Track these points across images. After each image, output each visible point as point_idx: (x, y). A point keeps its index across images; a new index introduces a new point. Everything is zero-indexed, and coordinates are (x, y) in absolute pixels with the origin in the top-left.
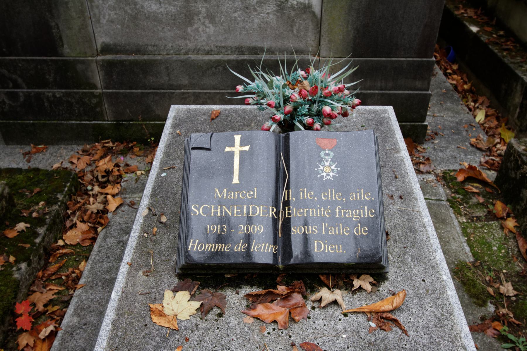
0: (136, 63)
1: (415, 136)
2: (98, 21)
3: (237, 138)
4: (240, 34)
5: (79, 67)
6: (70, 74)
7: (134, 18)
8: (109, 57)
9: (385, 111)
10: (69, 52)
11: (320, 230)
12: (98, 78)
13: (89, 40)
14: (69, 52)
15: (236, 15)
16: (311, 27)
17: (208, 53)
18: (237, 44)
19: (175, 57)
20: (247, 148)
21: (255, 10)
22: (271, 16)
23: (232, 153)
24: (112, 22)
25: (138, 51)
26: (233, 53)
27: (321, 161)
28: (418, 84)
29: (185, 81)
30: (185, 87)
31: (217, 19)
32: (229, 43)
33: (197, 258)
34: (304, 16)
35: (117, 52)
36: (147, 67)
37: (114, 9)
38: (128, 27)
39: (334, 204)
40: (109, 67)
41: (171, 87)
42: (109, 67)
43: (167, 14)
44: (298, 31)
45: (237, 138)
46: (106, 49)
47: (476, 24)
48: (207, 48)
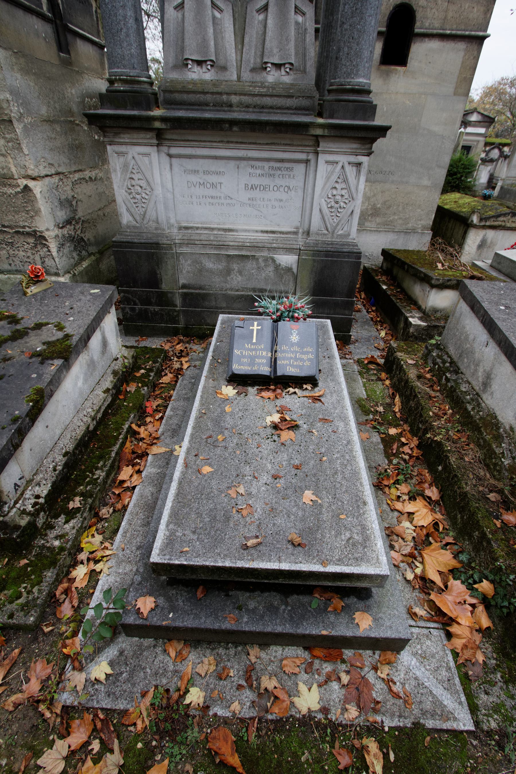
0: (199, 294)
1: (343, 339)
2: (182, 272)
3: (256, 323)
5: (169, 295)
6: (164, 299)
7: (200, 271)
8: (185, 291)
9: (326, 322)
10: (165, 287)
11: (290, 362)
12: (178, 301)
13: (176, 281)
14: (165, 287)
16: (292, 279)
17: (237, 291)
19: (220, 292)
20: (260, 328)
23: (253, 330)
24: (189, 272)
27: (292, 334)
28: (347, 312)
29: (224, 305)
30: (224, 308)
32: (249, 286)
33: (236, 372)
35: (189, 288)
36: (205, 297)
37: (190, 265)
39: (297, 352)
40: (185, 296)
41: (217, 308)
42: (185, 296)
44: (285, 281)
45: (256, 323)
46: (184, 286)
47: (385, 284)
48: (237, 288)
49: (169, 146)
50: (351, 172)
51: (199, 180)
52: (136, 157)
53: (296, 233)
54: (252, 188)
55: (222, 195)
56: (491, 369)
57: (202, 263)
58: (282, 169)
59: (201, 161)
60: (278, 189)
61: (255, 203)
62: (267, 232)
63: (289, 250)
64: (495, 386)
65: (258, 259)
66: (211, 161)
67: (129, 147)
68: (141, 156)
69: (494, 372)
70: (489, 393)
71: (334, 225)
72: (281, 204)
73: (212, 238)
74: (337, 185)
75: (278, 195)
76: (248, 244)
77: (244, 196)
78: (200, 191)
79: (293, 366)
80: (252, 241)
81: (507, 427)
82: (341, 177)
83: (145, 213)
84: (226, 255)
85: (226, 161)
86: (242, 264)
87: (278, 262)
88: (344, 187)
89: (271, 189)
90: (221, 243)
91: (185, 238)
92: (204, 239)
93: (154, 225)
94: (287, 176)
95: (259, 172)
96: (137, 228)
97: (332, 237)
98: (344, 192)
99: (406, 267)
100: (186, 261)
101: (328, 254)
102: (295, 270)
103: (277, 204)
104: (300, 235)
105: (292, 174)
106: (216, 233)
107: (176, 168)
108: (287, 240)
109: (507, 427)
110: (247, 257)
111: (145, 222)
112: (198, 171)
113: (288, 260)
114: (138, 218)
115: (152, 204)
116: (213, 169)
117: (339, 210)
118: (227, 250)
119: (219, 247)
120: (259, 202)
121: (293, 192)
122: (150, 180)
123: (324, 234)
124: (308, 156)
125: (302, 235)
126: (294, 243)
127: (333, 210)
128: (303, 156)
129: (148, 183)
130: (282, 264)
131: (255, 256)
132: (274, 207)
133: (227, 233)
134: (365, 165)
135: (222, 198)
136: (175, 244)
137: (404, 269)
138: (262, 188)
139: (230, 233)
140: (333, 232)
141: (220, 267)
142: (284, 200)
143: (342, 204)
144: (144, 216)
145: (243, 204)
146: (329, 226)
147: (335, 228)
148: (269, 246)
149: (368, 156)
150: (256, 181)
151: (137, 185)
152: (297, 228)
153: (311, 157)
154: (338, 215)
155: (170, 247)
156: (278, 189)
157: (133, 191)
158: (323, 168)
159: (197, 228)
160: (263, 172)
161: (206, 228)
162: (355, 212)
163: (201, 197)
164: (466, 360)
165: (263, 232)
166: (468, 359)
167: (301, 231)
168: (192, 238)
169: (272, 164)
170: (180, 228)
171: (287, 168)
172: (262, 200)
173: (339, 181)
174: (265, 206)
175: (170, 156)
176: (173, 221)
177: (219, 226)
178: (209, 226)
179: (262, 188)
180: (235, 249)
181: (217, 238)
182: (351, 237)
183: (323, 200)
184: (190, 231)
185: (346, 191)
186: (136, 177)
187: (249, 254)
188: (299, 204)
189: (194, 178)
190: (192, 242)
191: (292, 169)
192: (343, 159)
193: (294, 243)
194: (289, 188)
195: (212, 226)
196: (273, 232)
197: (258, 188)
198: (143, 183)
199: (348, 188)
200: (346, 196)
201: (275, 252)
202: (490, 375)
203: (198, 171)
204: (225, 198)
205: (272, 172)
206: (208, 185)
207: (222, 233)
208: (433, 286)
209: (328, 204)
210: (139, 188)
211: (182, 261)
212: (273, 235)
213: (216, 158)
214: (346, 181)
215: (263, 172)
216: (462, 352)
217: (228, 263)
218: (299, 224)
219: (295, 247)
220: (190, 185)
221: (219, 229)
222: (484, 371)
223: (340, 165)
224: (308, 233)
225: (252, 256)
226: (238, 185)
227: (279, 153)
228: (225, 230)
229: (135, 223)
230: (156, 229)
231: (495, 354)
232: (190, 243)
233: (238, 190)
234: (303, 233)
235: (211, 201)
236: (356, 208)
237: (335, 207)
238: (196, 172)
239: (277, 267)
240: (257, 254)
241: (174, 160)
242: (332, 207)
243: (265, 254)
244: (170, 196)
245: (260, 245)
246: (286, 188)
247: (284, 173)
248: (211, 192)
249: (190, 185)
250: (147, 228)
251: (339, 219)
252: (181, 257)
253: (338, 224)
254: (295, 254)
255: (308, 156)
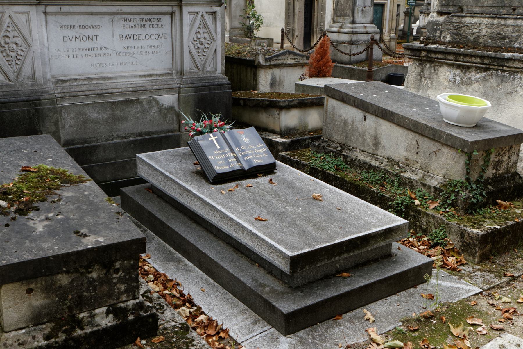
0: (92, 147)
2: (63, 127)
4: (141, 125)
7: (85, 123)
15: (138, 115)
16: (175, 118)
17: (125, 138)
18: (139, 131)
19: (108, 142)
21: (147, 111)
22: (156, 114)
24: (72, 126)
25: (85, 142)
26: (137, 136)
29: (113, 155)
30: (114, 159)
31: (129, 119)
32: (135, 131)
34: (171, 112)
35: (73, 144)
37: (74, 119)
38: (80, 129)
43: (103, 119)
44: (169, 120)
48: (124, 135)
49: (46, 5)
50: (209, 19)
51: (74, 34)
52: (13, 15)
53: (170, 74)
54: (126, 38)
55: (99, 47)
56: (376, 132)
57: (86, 115)
58: (152, 20)
59: (77, 17)
60: (150, 37)
61: (130, 51)
62: (144, 76)
63: (169, 90)
64: (383, 141)
65: (142, 102)
66: (86, 16)
67: (5, 7)
68: (17, 15)
69: (379, 132)
70: (381, 148)
71: (203, 63)
72: (154, 50)
73: (92, 88)
74: (199, 30)
75: (150, 42)
76: (131, 89)
77: (119, 46)
78: (76, 44)
79: (258, 159)
80: (133, 86)
81: (404, 160)
82: (202, 23)
83: (20, 70)
84: (111, 102)
85: (101, 16)
86: (127, 110)
87: (160, 103)
88: (206, 31)
89: (144, 37)
90: (104, 92)
91: (65, 91)
92: (85, 89)
93: (30, 82)
94: (156, 26)
95: (131, 23)
96: (11, 86)
97: (203, 73)
98: (206, 35)
99: (242, 102)
100: (69, 114)
101: (203, 88)
102: (176, 108)
103: (150, 50)
104: (174, 76)
105: (160, 24)
106: (95, 82)
107: (51, 26)
108: (165, 81)
109: (404, 160)
110: (131, 101)
111: (20, 80)
112: (74, 26)
113: (169, 99)
114: (12, 76)
115: (28, 61)
116: (89, 23)
117: (205, 50)
118: (110, 97)
119: (103, 95)
120: (133, 50)
121: (163, 39)
122: (27, 37)
123: (196, 72)
124: (173, 9)
125: (176, 76)
126: (171, 82)
127: (200, 51)
128: (169, 9)
129: (24, 39)
130: (164, 103)
131: (139, 99)
132: (147, 53)
133: (107, 82)
134: (219, 13)
135: (99, 49)
136: (57, 98)
137: (239, 104)
138: (135, 37)
139: (110, 81)
140: (203, 69)
141: (105, 116)
142: (156, 46)
143: (207, 45)
144: (18, 74)
145: (118, 53)
146: (199, 65)
147: (204, 65)
148: (150, 88)
149: (220, 6)
150: (129, 32)
151: (12, 43)
152: (170, 70)
153: (176, 9)
154: (204, 54)
155: (53, 101)
156: (150, 37)
157: (7, 49)
158: (187, 18)
159: (76, 80)
160: (135, 24)
161: (84, 79)
162: (217, 50)
163: (77, 50)
164: (352, 138)
165: (140, 76)
166: (354, 136)
167: (174, 72)
168: (72, 90)
169: (142, 16)
170: (57, 82)
171: (156, 20)
172: (136, 47)
173: (201, 26)
174: (139, 53)
175: (45, 13)
176: (48, 76)
177: (97, 76)
178: (87, 76)
179: (135, 37)
180: (119, 95)
181: (98, 87)
182: (218, 72)
183: (191, 43)
184: (68, 84)
185: (207, 34)
186: (11, 35)
187: (132, 98)
188: (169, 49)
189: (70, 33)
190: (74, 94)
191: (160, 20)
192: (202, 10)
193: (171, 82)
194: (159, 35)
195: (91, 76)
196: (150, 76)
197: (132, 38)
198: (19, 41)
199: (209, 32)
200: (208, 38)
201: (157, 93)
202: (377, 136)
203: (74, 26)
204: (102, 49)
205: (142, 23)
206: (85, 39)
207: (102, 82)
208: (281, 108)
209: (194, 46)
210: (15, 46)
211: (64, 115)
212: (151, 79)
213: (92, 14)
214: (206, 26)
215: (135, 24)
216: (347, 133)
217: (113, 111)
218: (171, 66)
219: (174, 86)
220: (65, 39)
221: (98, 79)
222: (371, 136)
223: (200, 14)
224: (181, 73)
225: (137, 99)
226: (113, 36)
227: (165, 7)
228: (104, 79)
229: (7, 81)
230: (33, 85)
231: (374, 121)
232: (72, 95)
233: (113, 40)
234: (177, 73)
235: (88, 52)
236: (218, 47)
237: (202, 48)
238: (72, 27)
239: (160, 107)
240: (141, 98)
241: (49, 17)
242: (198, 48)
243: (148, 96)
244: (46, 51)
245: (142, 89)
246: (157, 36)
247: (153, 23)
248: (88, 44)
249: (65, 39)
250: (22, 85)
251: (206, 58)
252: (63, 111)
253: (205, 62)
254: (175, 92)
255: (173, 9)
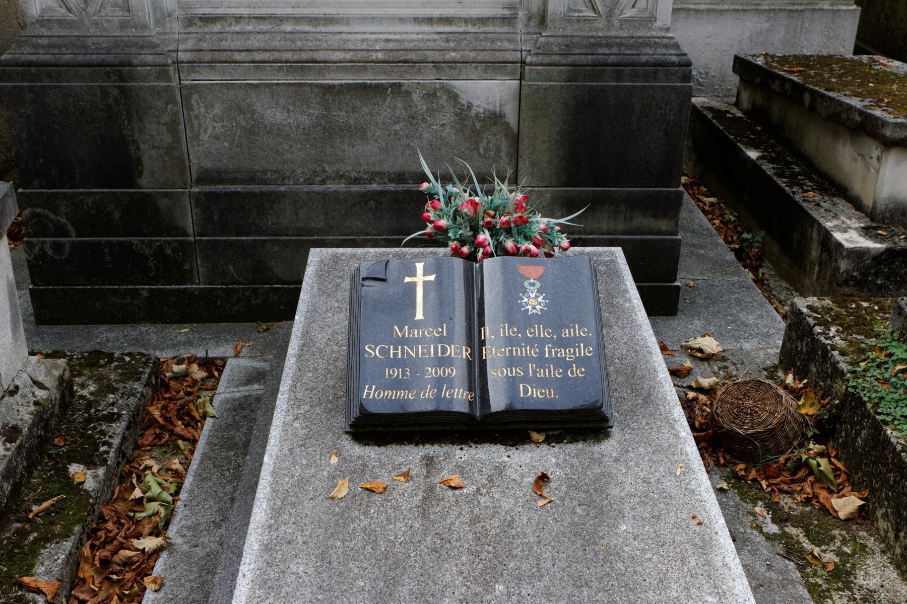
1: (662, 302)
2: (196, 137)
3: (420, 266)
4: (403, 154)
5: (163, 203)
6: (146, 214)
7: (250, 132)
8: (208, 188)
9: (612, 254)
11: (526, 371)
12: (189, 221)
13: (181, 164)
14: (147, 184)
15: (397, 127)
16: (504, 146)
17: (357, 181)
18: (398, 168)
19: (306, 188)
20: (432, 278)
21: (424, 119)
22: (448, 129)
23: (413, 285)
24: (217, 138)
25: (252, 180)
26: (391, 181)
27: (525, 291)
28: (664, 225)
30: (320, 231)
31: (369, 134)
32: (386, 167)
33: (372, 409)
34: (494, 129)
35: (221, 182)
36: (266, 202)
37: (222, 119)
38: (240, 145)
39: (542, 342)
40: (206, 202)
41: (299, 232)
42: (206, 202)
43: (298, 126)
44: (487, 149)
45: (420, 266)
46: (205, 177)
47: (756, 147)
48: (354, 175)
57: (253, 112)
62: (430, 20)
63: (493, 67)
65: (408, 94)
73: (276, 44)
76: (380, 56)
80: (391, 46)
86: (365, 110)
90: (304, 56)
91: (204, 45)
93: (117, 15)
96: (70, 25)
99: (807, 97)
100: (209, 106)
101: (598, 69)
104: (520, 26)
106: (288, 28)
108: (486, 39)
110: (379, 89)
111: (91, 9)
113: (490, 93)
118: (321, 73)
119: (301, 66)
123: (587, 20)
126: (506, 45)
130: (475, 103)
131: (400, 85)
133: (321, 29)
136: (177, 62)
137: (801, 102)
139: (330, 29)
140: (610, 14)
141: (305, 120)
148: (437, 56)
152: (511, 7)
159: (239, 19)
161: (261, 18)
165: (417, 20)
167: (521, 14)
168: (224, 45)
170: (190, 21)
177: (297, 11)
178: (270, 11)
180: (346, 70)
182: (658, 23)
184: (217, 28)
187: (383, 80)
190: (223, 56)
193: (506, 45)
195: (279, 12)
196: (447, 21)
201: (455, 72)
208: (889, 144)
211: (198, 108)
212: (448, 29)
217: (327, 109)
219: (508, 56)
221: (298, 20)
224: (542, 19)
228: (313, 20)
229: (63, 11)
230: (123, 25)
232: (218, 59)
234: (529, 19)
239: (463, 112)
240: (407, 81)
243: (428, 78)
245: (412, 56)
250: (96, 24)
252: (195, 97)
254: (511, 75)
